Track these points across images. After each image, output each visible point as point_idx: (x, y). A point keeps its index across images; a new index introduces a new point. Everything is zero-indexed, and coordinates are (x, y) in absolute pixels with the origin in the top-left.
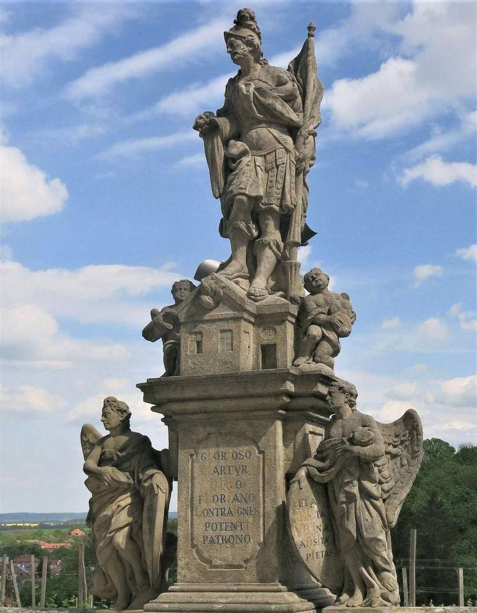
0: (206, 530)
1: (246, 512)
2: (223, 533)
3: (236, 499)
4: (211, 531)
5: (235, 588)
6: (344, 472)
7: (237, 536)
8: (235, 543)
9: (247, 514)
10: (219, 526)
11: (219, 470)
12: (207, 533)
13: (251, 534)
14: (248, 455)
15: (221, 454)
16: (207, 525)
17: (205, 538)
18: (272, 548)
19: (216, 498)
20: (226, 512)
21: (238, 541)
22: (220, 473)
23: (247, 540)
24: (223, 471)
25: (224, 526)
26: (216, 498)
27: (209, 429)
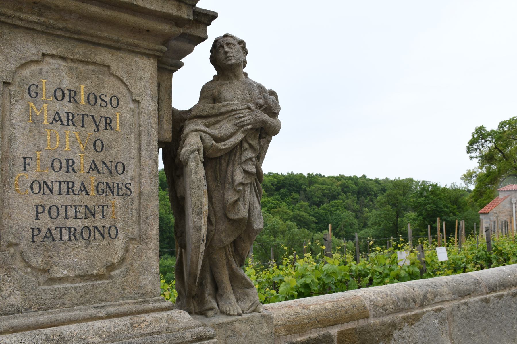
0: (37, 218)
1: (110, 189)
2: (70, 222)
3: (94, 168)
4: (48, 220)
5: (102, 313)
6: (246, 145)
7: (96, 228)
8: (92, 238)
9: (113, 193)
10: (62, 211)
11: (64, 120)
12: (37, 224)
13: (119, 225)
14: (114, 103)
15: (67, 93)
16: (39, 209)
17: (35, 231)
18: (152, 245)
19: (57, 164)
20: (76, 188)
21: (98, 235)
22: (65, 123)
23: (113, 234)
24: (70, 121)
25: (71, 212)
26: (57, 164)
27: (47, 49)
